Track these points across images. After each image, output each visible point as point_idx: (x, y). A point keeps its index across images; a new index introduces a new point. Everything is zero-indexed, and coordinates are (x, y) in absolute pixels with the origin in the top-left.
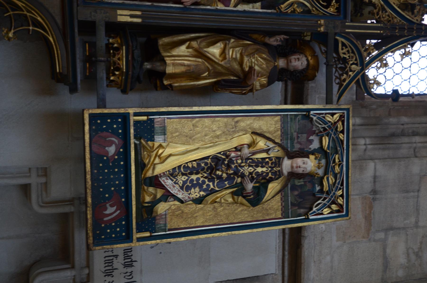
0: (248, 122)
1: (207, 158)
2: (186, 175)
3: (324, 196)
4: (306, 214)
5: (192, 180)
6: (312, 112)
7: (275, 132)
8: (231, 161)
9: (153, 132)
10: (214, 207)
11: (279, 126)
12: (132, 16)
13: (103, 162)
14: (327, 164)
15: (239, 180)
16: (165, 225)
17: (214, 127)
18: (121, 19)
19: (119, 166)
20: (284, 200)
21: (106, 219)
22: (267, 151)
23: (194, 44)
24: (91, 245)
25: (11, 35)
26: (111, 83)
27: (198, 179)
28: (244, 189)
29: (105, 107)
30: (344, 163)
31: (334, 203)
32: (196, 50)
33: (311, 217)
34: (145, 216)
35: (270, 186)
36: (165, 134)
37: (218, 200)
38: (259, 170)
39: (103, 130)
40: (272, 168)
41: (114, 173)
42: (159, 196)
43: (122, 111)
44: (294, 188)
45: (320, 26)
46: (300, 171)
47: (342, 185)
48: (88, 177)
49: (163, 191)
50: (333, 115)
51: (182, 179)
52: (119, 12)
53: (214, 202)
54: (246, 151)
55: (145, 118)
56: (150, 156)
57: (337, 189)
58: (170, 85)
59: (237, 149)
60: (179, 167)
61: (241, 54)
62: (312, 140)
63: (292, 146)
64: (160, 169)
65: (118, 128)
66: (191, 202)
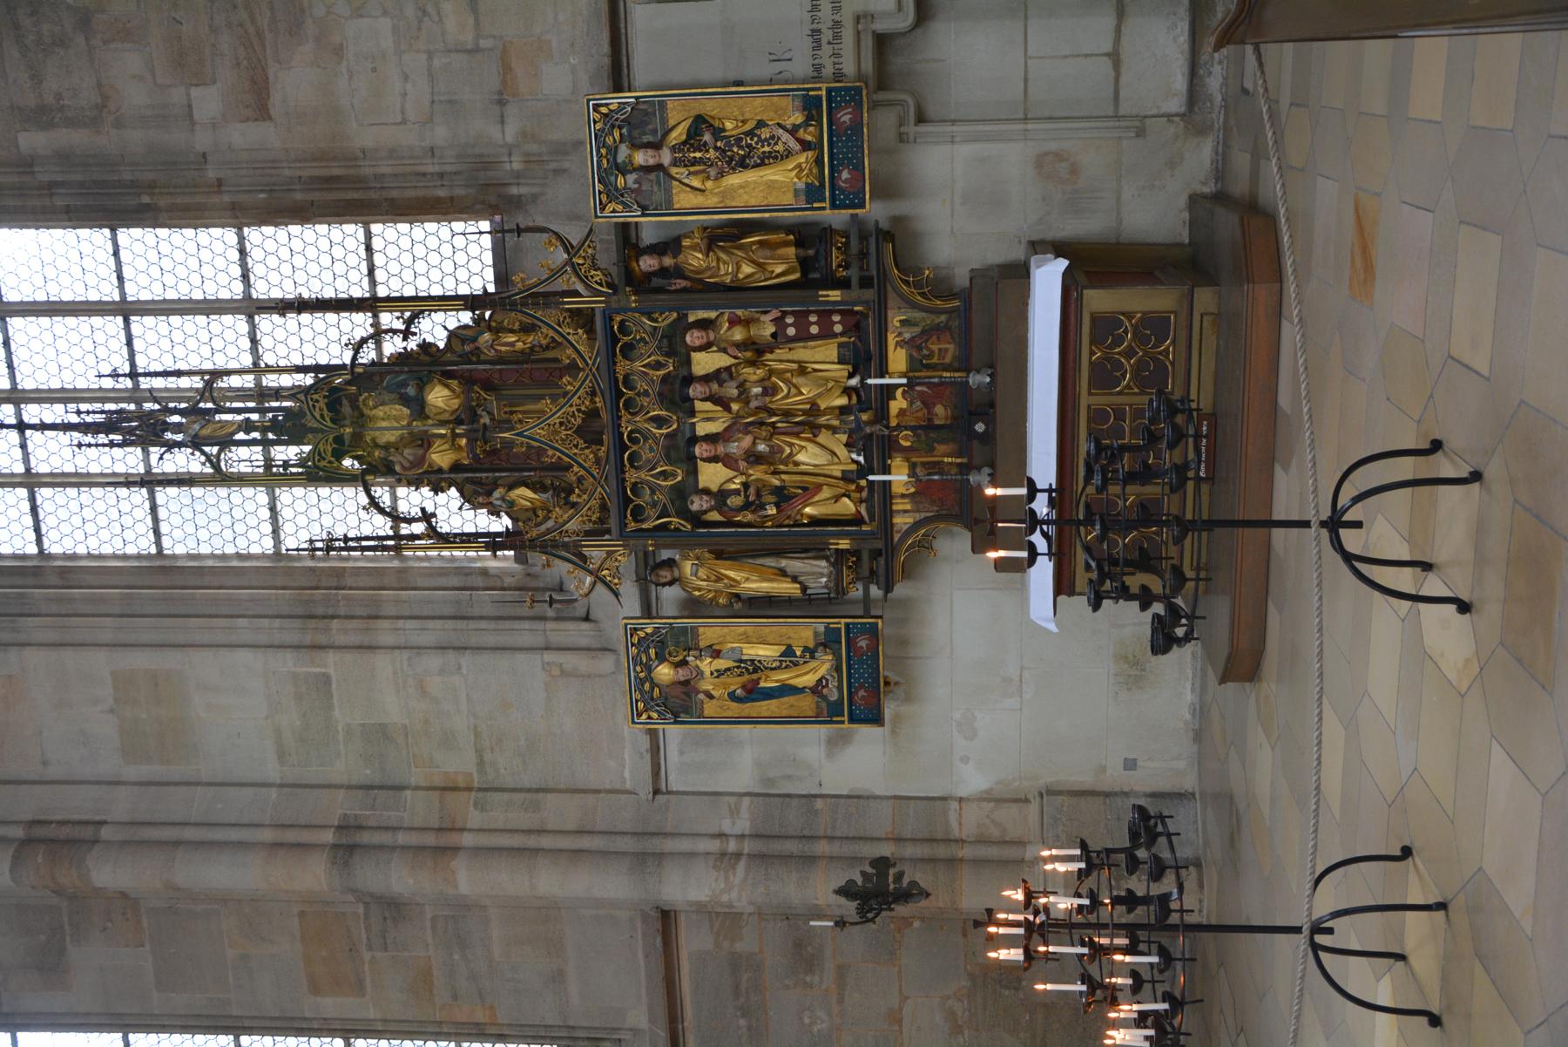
0: (709, 201)
1: (753, 167)
2: (776, 151)
3: (617, 123)
4: (637, 103)
5: (768, 145)
6: (639, 213)
7: (679, 192)
8: (729, 163)
9: (807, 192)
10: (743, 115)
11: (675, 199)
12: (828, 296)
13: (853, 164)
14: (615, 159)
15: (719, 144)
16: (793, 100)
17: (746, 197)
18: (837, 293)
19: (838, 160)
20: (664, 120)
21: (850, 110)
22: (690, 174)
23: (768, 275)
24: (864, 87)
25: (927, 272)
26: (846, 234)
27: (763, 146)
28: (713, 134)
29: (852, 215)
30: (595, 159)
31: (606, 115)
32: (765, 269)
33: (633, 100)
34: (814, 112)
35: (684, 137)
36: (795, 190)
37: (740, 124)
38: (698, 155)
39: (853, 194)
40: (684, 156)
41: (843, 153)
42: (802, 131)
43: (836, 211)
44: (655, 131)
45: (635, 301)
46: (650, 152)
47: (596, 134)
48: (866, 152)
49: (798, 136)
50: (613, 212)
51: (779, 147)
52: (839, 299)
53: (744, 122)
54: (713, 172)
55: (815, 205)
56: (810, 170)
57: (602, 130)
58: (787, 235)
59: (721, 174)
60: (782, 159)
61: (719, 268)
62: (634, 183)
63: (658, 177)
64: (802, 158)
65: (839, 195)
66: (770, 123)
